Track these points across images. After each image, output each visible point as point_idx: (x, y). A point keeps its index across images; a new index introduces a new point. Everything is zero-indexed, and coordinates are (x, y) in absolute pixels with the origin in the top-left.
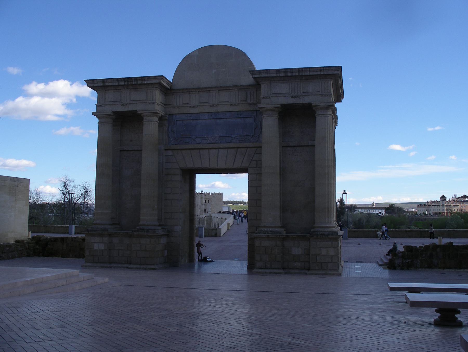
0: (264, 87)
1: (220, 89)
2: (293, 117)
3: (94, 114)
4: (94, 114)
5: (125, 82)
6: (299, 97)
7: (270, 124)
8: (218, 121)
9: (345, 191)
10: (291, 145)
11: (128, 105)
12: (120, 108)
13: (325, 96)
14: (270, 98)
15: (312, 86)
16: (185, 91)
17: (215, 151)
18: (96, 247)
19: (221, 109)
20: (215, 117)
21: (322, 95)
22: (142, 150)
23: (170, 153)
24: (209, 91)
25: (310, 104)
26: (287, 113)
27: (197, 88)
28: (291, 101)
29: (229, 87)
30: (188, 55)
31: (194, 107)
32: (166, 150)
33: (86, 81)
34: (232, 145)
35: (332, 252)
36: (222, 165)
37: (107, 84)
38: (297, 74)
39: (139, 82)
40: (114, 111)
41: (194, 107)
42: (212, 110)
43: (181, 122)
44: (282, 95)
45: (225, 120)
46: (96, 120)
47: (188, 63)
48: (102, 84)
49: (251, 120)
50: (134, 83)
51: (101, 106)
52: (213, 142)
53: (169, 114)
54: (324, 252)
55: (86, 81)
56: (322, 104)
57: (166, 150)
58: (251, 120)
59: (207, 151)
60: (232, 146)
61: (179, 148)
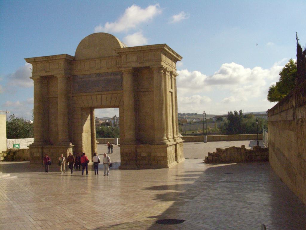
0: (123, 57)
1: (101, 58)
2: (142, 74)
3: (31, 78)
4: (31, 78)
5: (46, 59)
6: (143, 63)
7: (127, 80)
9: (204, 112)
11: (49, 72)
12: (44, 74)
17: (100, 96)
18: (35, 155)
19: (102, 71)
22: (57, 97)
23: (75, 98)
26: (137, 73)
27: (89, 59)
28: (138, 66)
29: (106, 57)
32: (73, 97)
33: (25, 59)
34: (109, 92)
35: (163, 155)
36: (104, 104)
37: (36, 60)
38: (141, 49)
39: (54, 59)
40: (42, 75)
42: (98, 71)
43: (81, 80)
44: (134, 62)
45: (105, 77)
47: (84, 44)
48: (34, 61)
49: (119, 77)
51: (34, 73)
54: (159, 155)
55: (25, 59)
57: (73, 97)
58: (119, 77)
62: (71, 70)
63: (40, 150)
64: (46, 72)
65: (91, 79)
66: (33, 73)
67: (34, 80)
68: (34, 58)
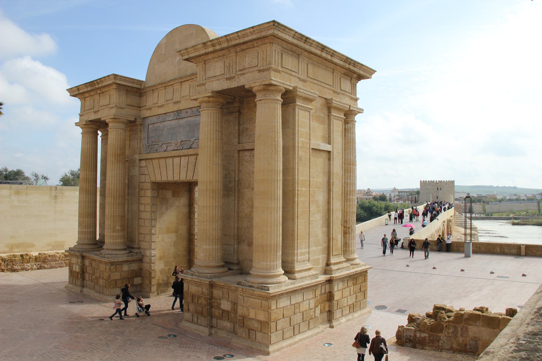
8: (182, 122)
10: (247, 148)
12: (93, 117)
13: (263, 71)
14: (204, 84)
15: (249, 59)
16: (154, 88)
20: (178, 117)
21: (260, 71)
23: (143, 163)
24: (173, 84)
25: (242, 88)
30: (158, 45)
31: (162, 106)
32: (140, 160)
35: (261, 317)
41: (162, 106)
42: (176, 108)
45: (187, 119)
46: (79, 130)
47: (159, 55)
48: (77, 92)
50: (97, 86)
52: (175, 148)
53: (144, 118)
56: (257, 84)
57: (140, 160)
59: (172, 159)
60: (190, 153)
61: (149, 157)
62: (140, 107)
63: (79, 260)
64: (95, 112)
65: (166, 123)
66: (81, 115)
67: (82, 128)
68: (76, 87)
